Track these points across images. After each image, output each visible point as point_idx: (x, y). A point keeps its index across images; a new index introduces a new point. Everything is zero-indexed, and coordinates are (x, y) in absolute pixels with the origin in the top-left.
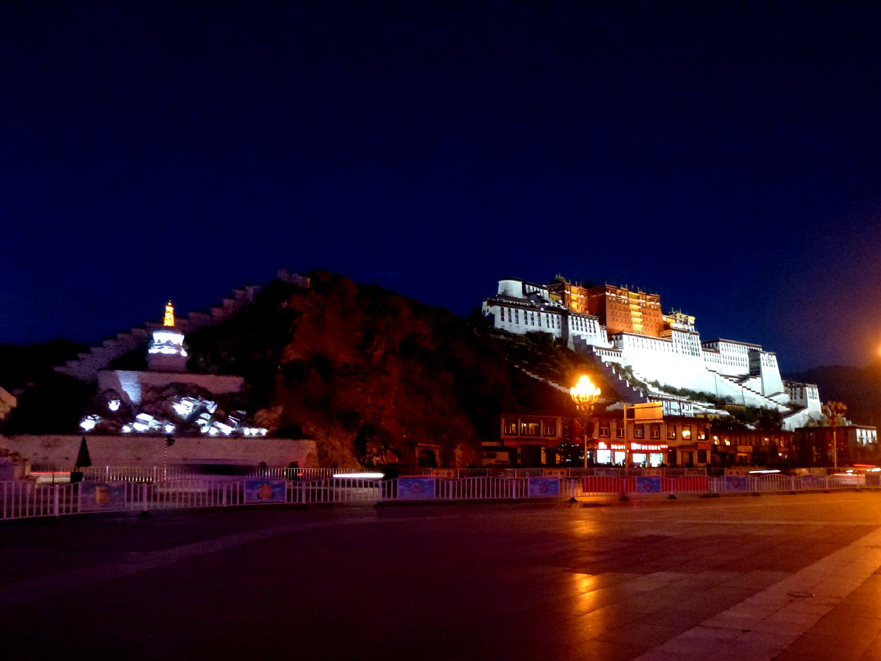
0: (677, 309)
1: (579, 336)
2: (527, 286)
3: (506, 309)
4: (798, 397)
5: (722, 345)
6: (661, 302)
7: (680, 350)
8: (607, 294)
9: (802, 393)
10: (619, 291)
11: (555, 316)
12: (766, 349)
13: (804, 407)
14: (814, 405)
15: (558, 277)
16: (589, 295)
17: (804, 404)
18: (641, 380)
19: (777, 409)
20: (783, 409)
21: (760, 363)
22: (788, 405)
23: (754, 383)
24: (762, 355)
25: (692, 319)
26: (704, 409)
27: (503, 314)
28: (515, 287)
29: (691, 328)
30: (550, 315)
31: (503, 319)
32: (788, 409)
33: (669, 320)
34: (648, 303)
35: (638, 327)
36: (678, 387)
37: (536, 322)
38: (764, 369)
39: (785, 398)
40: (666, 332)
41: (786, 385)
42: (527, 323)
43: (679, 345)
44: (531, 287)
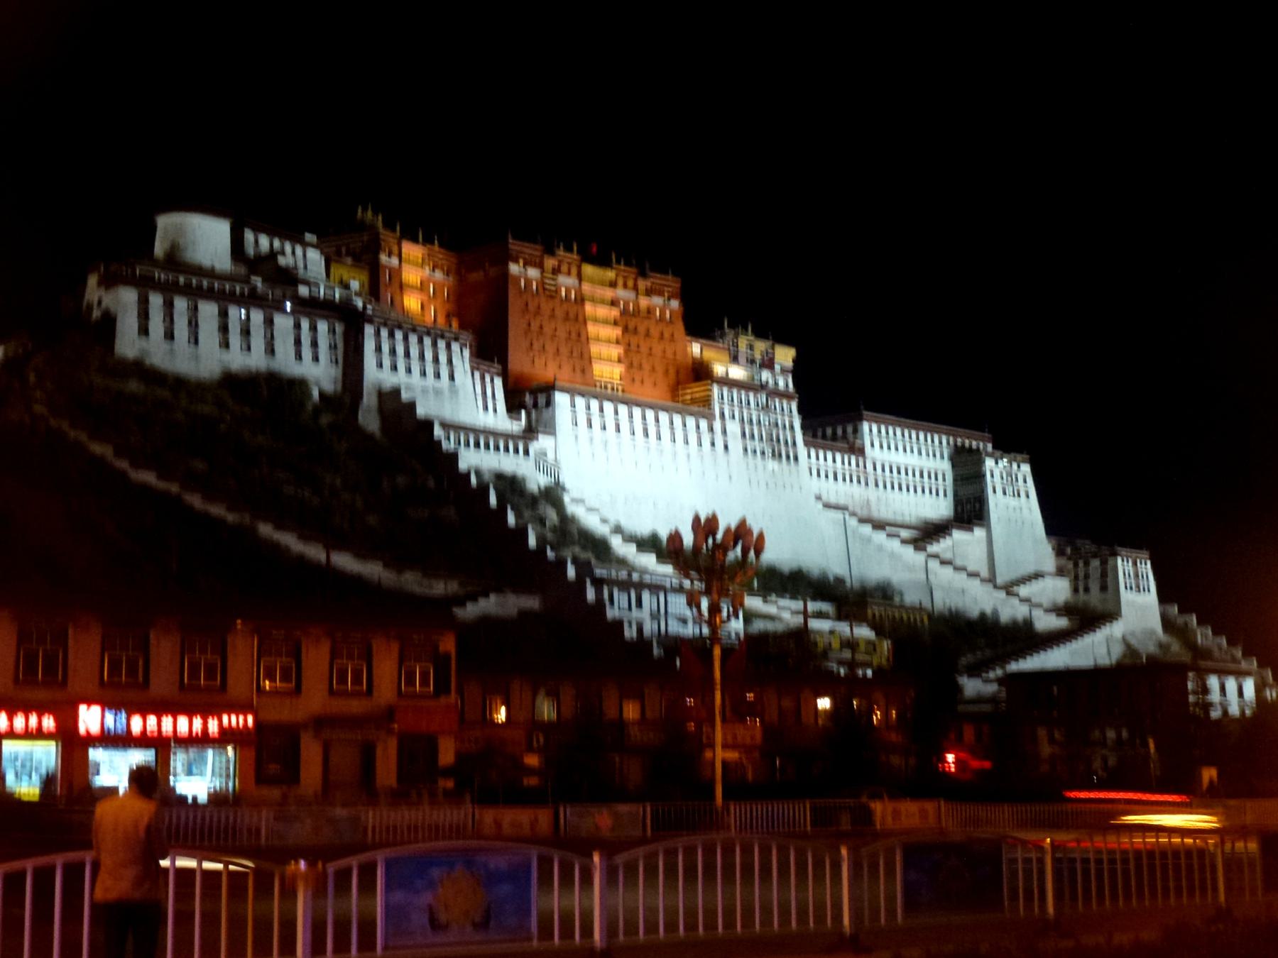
0: (739, 324)
1: (396, 392)
3: (156, 300)
4: (1095, 587)
5: (870, 431)
7: (736, 444)
8: (514, 268)
9: (1104, 575)
10: (550, 263)
13: (1110, 614)
14: (1139, 605)
16: (460, 271)
17: (1110, 606)
18: (592, 522)
19: (1028, 623)
20: (1046, 622)
21: (983, 490)
22: (1060, 610)
24: (989, 463)
25: (785, 356)
27: (144, 315)
28: (208, 238)
29: (785, 382)
30: (305, 324)
31: (144, 331)
34: (644, 302)
35: (608, 370)
37: (258, 341)
38: (998, 504)
39: (1057, 589)
40: (696, 390)
41: (1059, 552)
42: (225, 344)
43: (734, 427)
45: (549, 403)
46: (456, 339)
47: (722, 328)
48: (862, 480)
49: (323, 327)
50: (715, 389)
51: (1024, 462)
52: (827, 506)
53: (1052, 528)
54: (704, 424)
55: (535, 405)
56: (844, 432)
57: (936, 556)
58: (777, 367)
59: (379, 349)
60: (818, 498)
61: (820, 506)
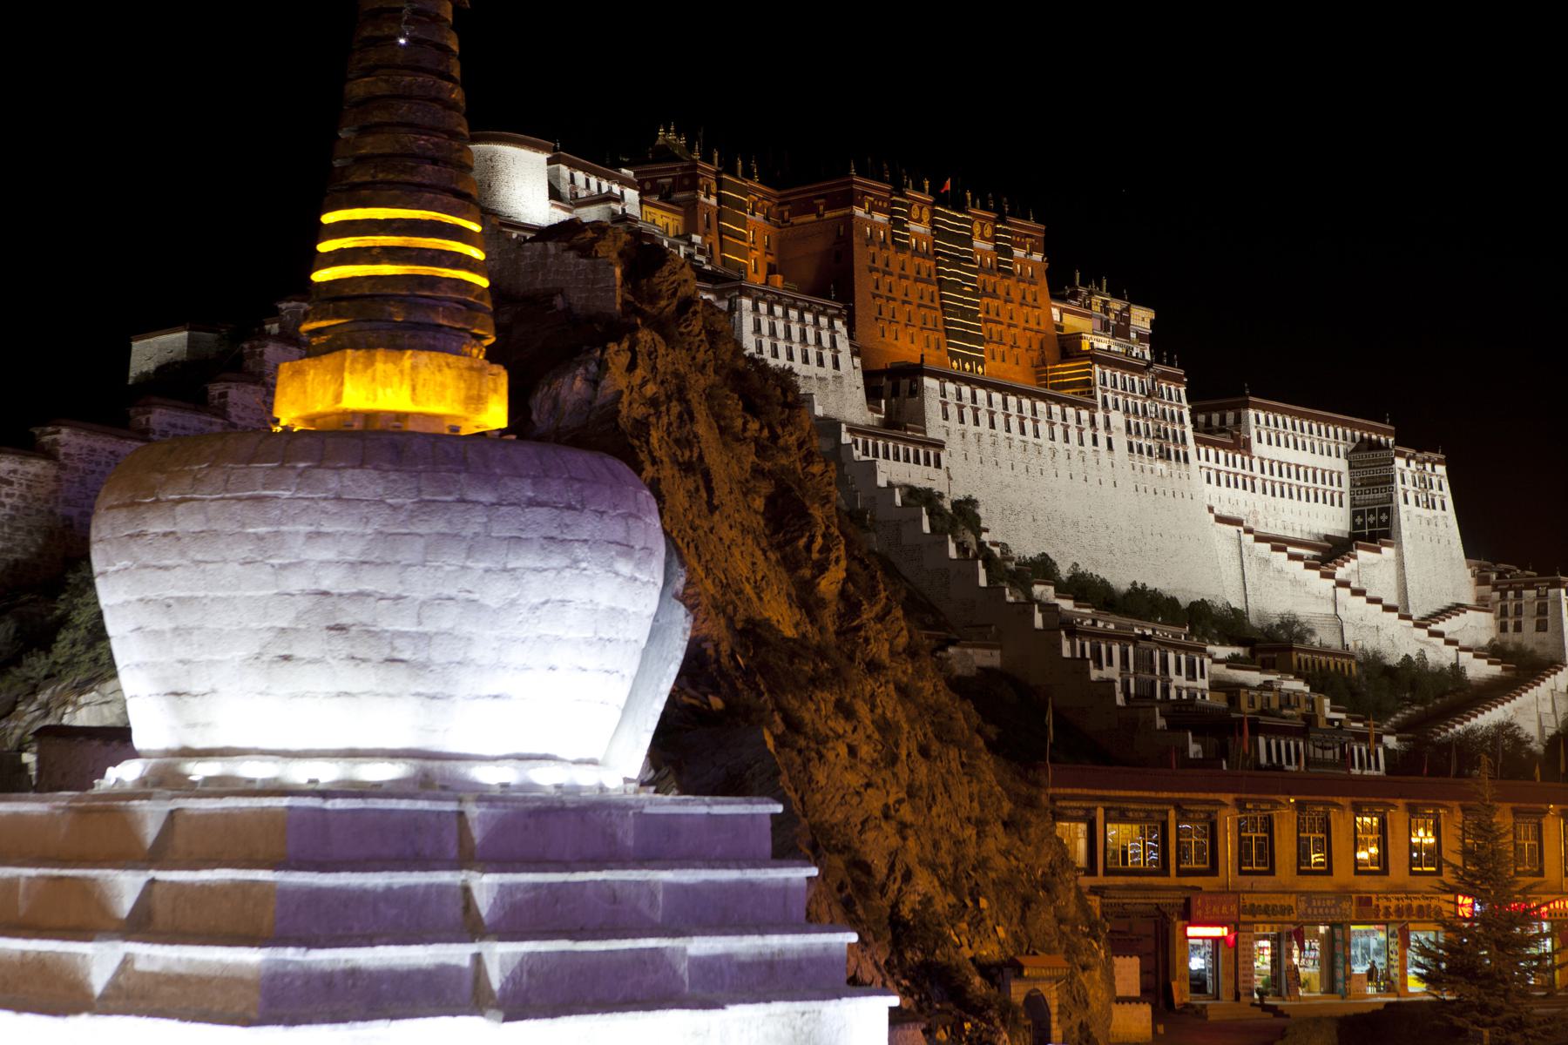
2: (565, 171)
4: (1529, 625)
5: (1255, 419)
6: (1047, 253)
7: (1120, 440)
8: (859, 212)
9: (1542, 611)
12: (1416, 440)
15: (666, 136)
19: (1457, 669)
20: (1479, 669)
22: (1493, 652)
24: (1400, 462)
25: (1142, 318)
26: (1221, 669)
32: (1496, 670)
33: (1072, 323)
36: (1121, 579)
38: (1409, 516)
39: (1478, 627)
40: (1068, 370)
41: (1482, 580)
43: (1118, 419)
44: (580, 176)
45: (917, 391)
46: (839, 316)
47: (1072, 284)
48: (1248, 484)
50: (1097, 369)
51: (1440, 462)
52: (1221, 519)
53: (1472, 545)
54: (1085, 414)
55: (895, 392)
56: (1223, 420)
57: (1344, 584)
58: (1133, 335)
59: (757, 329)
60: (1211, 509)
61: (1212, 516)
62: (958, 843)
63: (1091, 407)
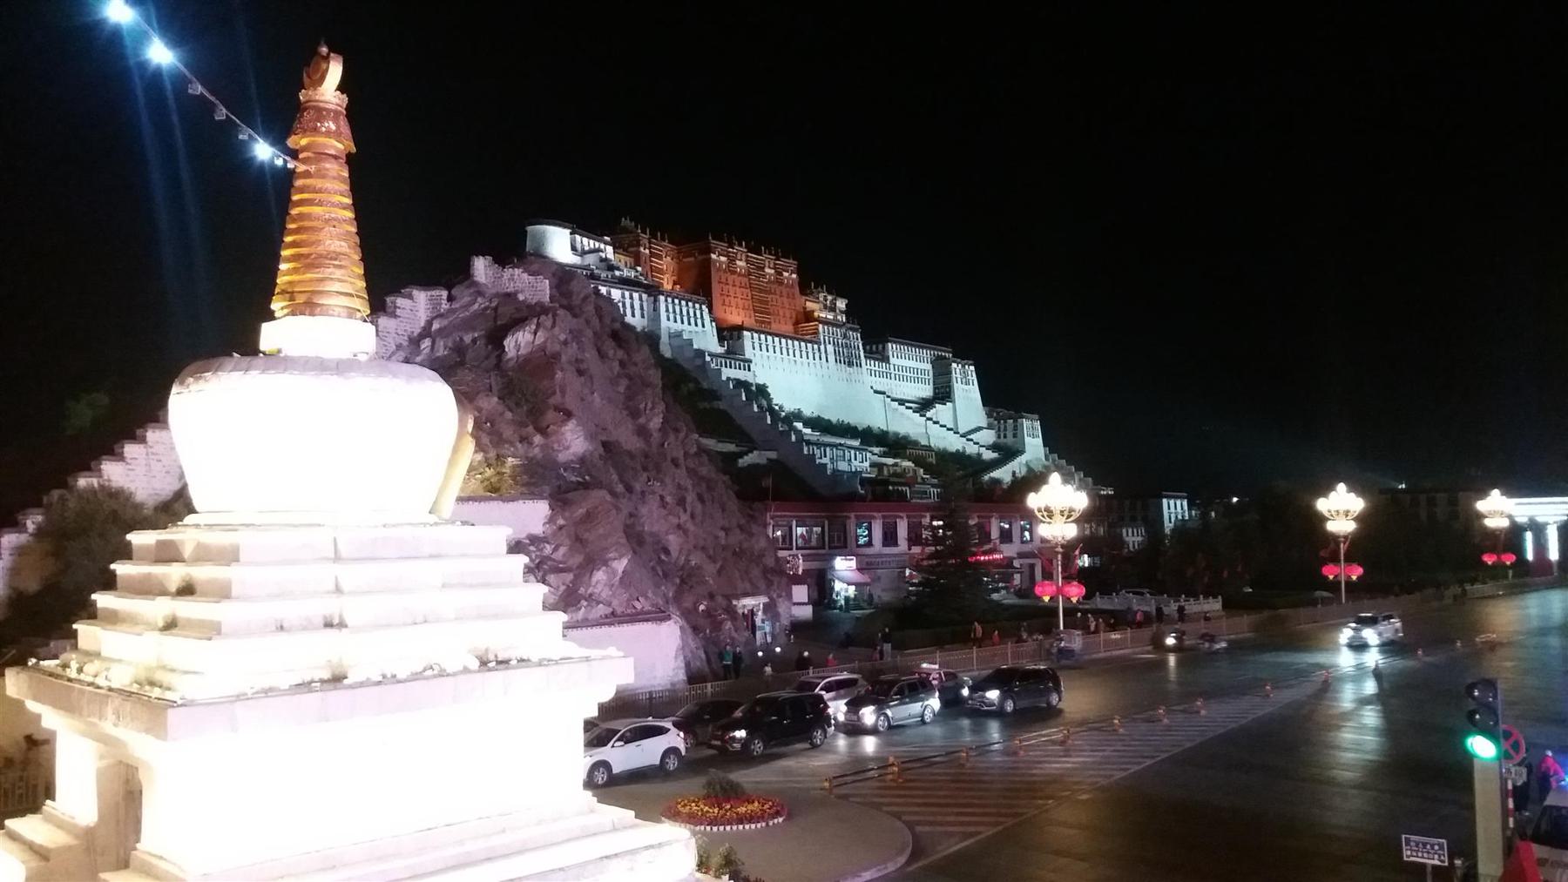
2: (578, 237)
4: (1010, 434)
7: (832, 358)
8: (714, 256)
9: (1015, 428)
11: (636, 295)
12: (961, 356)
13: (1021, 452)
19: (979, 455)
20: (989, 455)
21: (950, 381)
23: (941, 411)
25: (841, 304)
29: (842, 318)
32: (995, 455)
38: (959, 389)
39: (988, 437)
41: (989, 415)
43: (830, 348)
44: (585, 240)
45: (740, 337)
48: (888, 375)
49: (636, 295)
62: (717, 537)
63: (819, 343)
